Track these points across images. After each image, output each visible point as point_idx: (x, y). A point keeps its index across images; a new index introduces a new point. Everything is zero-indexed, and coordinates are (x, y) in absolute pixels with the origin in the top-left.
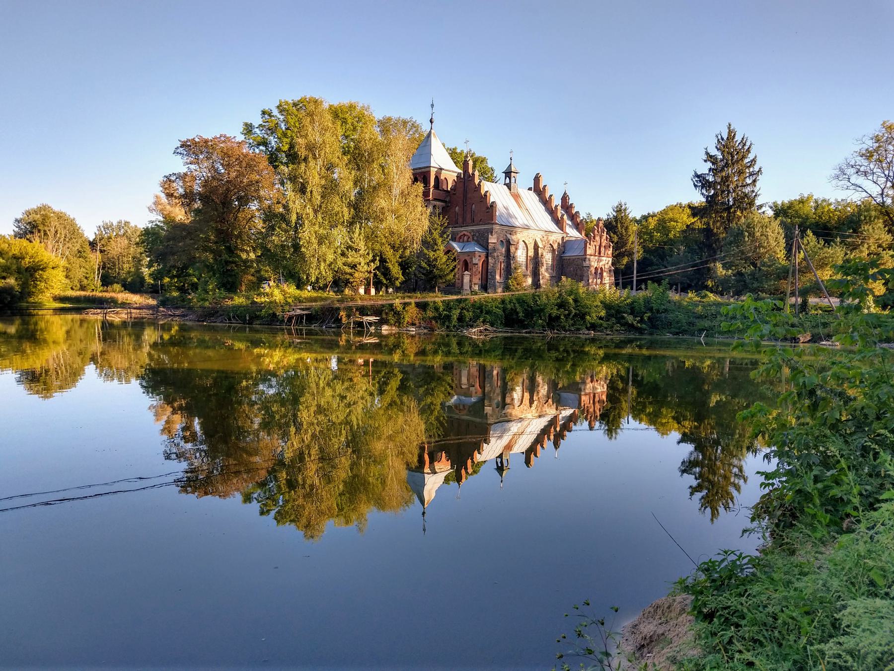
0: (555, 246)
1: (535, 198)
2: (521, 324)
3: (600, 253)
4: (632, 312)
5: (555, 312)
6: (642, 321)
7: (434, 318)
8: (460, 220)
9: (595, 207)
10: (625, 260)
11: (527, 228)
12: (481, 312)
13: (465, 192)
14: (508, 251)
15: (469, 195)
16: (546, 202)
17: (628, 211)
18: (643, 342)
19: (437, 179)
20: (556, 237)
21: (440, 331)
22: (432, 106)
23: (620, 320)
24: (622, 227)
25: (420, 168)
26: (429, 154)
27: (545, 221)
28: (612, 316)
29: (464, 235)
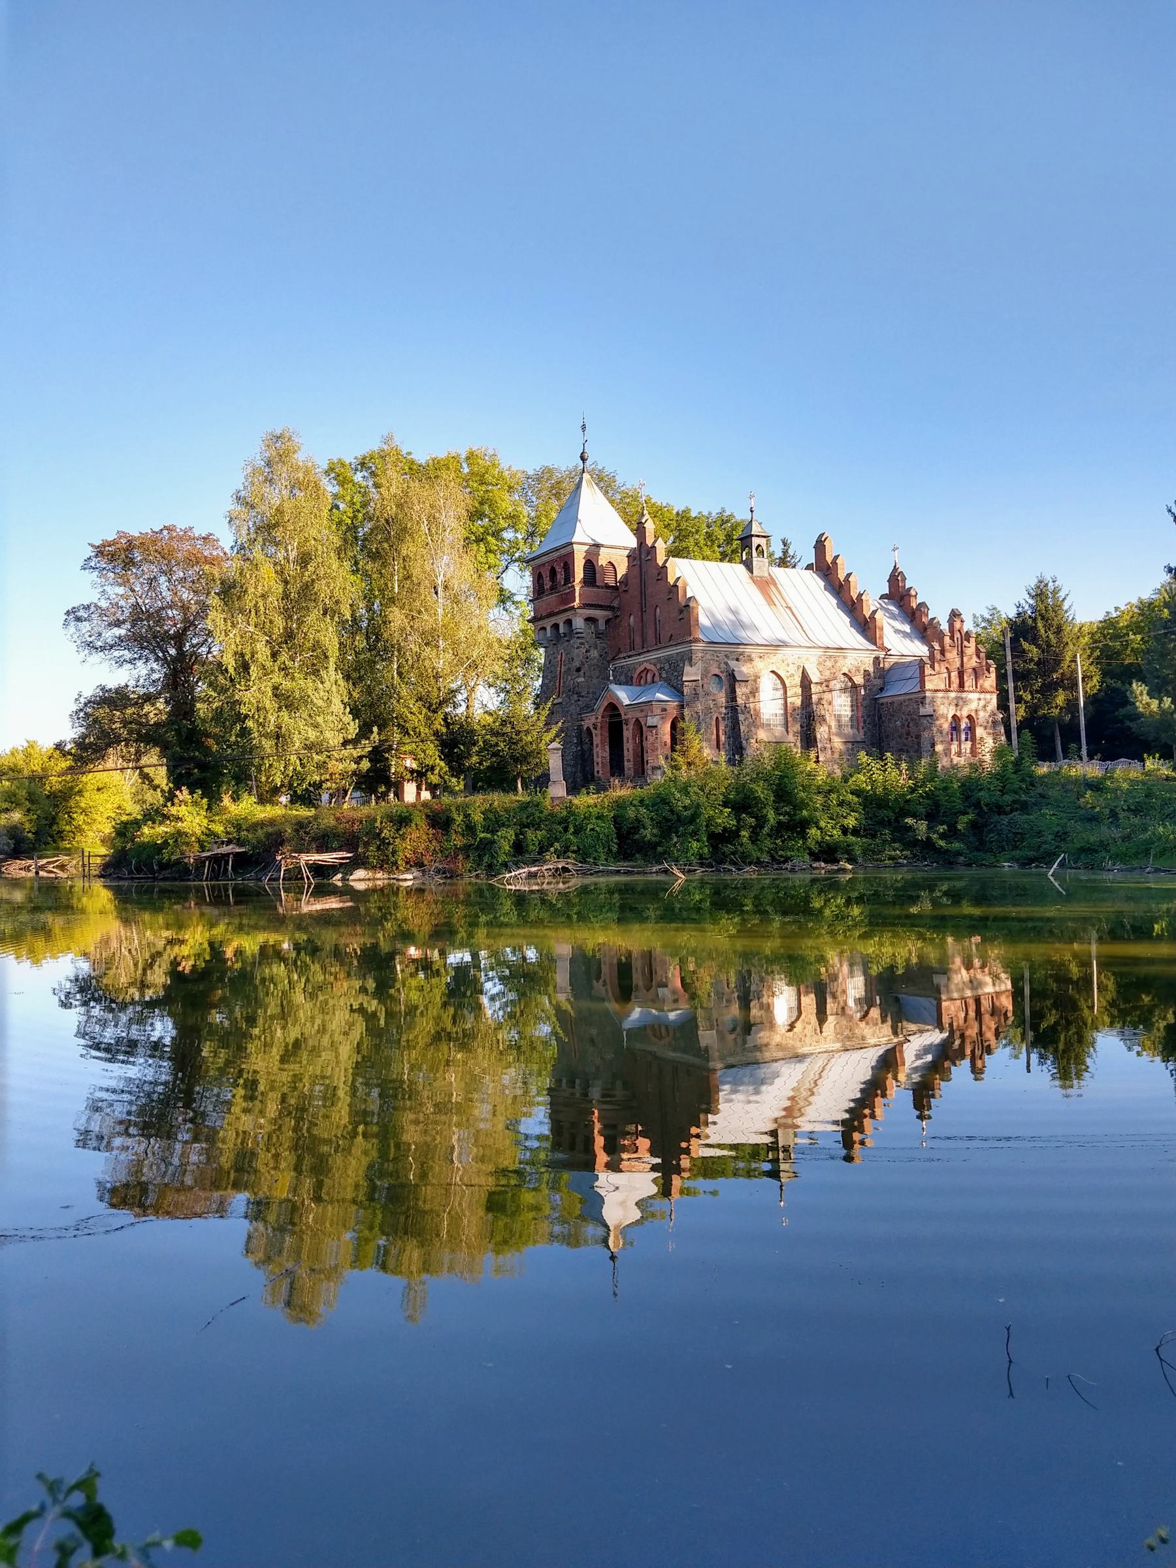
0: (859, 680)
1: (815, 582)
2: (652, 852)
3: (961, 685)
4: (931, 818)
5: (724, 819)
6: (952, 834)
7: (466, 849)
8: (638, 640)
9: (977, 591)
10: (1060, 698)
11: (778, 645)
12: (566, 829)
13: (643, 584)
14: (732, 696)
15: (649, 590)
16: (839, 588)
17: (1062, 594)
18: (959, 884)
19: (590, 566)
20: (859, 657)
21: (469, 880)
22: (584, 427)
23: (903, 835)
24: (1048, 627)
25: (556, 550)
26: (576, 519)
27: (836, 627)
28: (883, 823)
29: (646, 670)
